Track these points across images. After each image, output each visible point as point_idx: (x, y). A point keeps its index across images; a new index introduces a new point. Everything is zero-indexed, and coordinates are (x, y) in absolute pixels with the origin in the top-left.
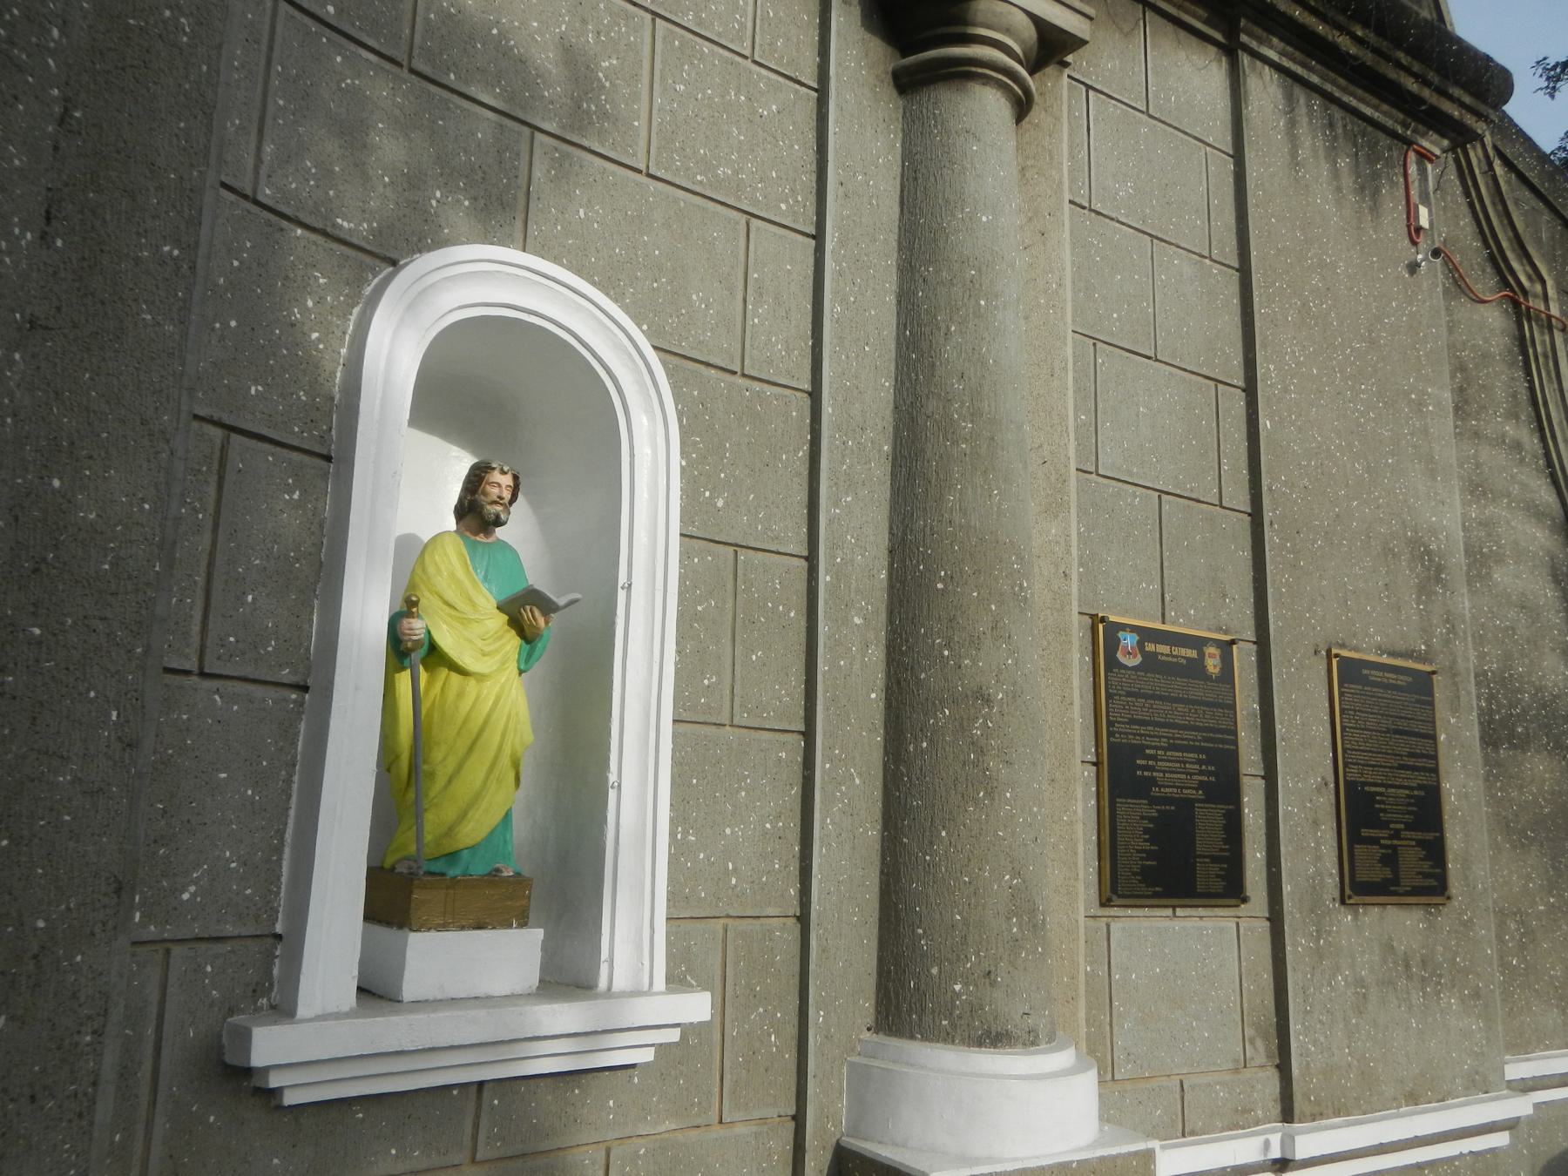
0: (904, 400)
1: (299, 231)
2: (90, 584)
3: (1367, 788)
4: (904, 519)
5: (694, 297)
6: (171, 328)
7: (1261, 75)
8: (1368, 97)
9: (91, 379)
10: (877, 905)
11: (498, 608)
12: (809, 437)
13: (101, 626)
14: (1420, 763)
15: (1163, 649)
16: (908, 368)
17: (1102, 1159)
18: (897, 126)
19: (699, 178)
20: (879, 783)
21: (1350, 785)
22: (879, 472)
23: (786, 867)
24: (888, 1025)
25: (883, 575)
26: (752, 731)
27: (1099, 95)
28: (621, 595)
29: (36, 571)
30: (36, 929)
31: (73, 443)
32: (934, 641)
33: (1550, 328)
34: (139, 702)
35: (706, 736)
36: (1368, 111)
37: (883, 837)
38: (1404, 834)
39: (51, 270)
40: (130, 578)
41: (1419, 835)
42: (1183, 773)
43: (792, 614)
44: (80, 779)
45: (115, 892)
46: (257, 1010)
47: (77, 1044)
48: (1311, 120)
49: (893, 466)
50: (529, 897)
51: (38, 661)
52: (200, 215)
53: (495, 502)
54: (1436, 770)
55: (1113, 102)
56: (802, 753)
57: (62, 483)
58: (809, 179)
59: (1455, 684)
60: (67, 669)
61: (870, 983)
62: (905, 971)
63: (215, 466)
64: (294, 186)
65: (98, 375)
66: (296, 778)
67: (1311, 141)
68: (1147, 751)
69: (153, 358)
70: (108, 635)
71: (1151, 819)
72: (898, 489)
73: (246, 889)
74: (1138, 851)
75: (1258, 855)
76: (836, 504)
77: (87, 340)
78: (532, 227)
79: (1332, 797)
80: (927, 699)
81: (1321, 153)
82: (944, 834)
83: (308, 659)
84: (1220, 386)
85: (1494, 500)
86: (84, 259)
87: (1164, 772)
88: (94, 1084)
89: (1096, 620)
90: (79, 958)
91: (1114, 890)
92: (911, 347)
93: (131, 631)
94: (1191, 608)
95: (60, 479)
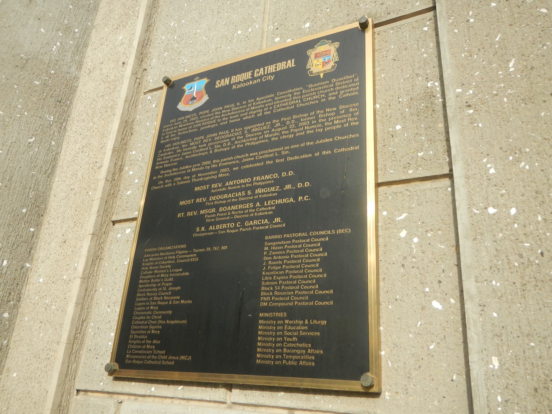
42: (250, 201)
68: (196, 189)
71: (185, 266)
75: (436, 304)
87: (217, 207)
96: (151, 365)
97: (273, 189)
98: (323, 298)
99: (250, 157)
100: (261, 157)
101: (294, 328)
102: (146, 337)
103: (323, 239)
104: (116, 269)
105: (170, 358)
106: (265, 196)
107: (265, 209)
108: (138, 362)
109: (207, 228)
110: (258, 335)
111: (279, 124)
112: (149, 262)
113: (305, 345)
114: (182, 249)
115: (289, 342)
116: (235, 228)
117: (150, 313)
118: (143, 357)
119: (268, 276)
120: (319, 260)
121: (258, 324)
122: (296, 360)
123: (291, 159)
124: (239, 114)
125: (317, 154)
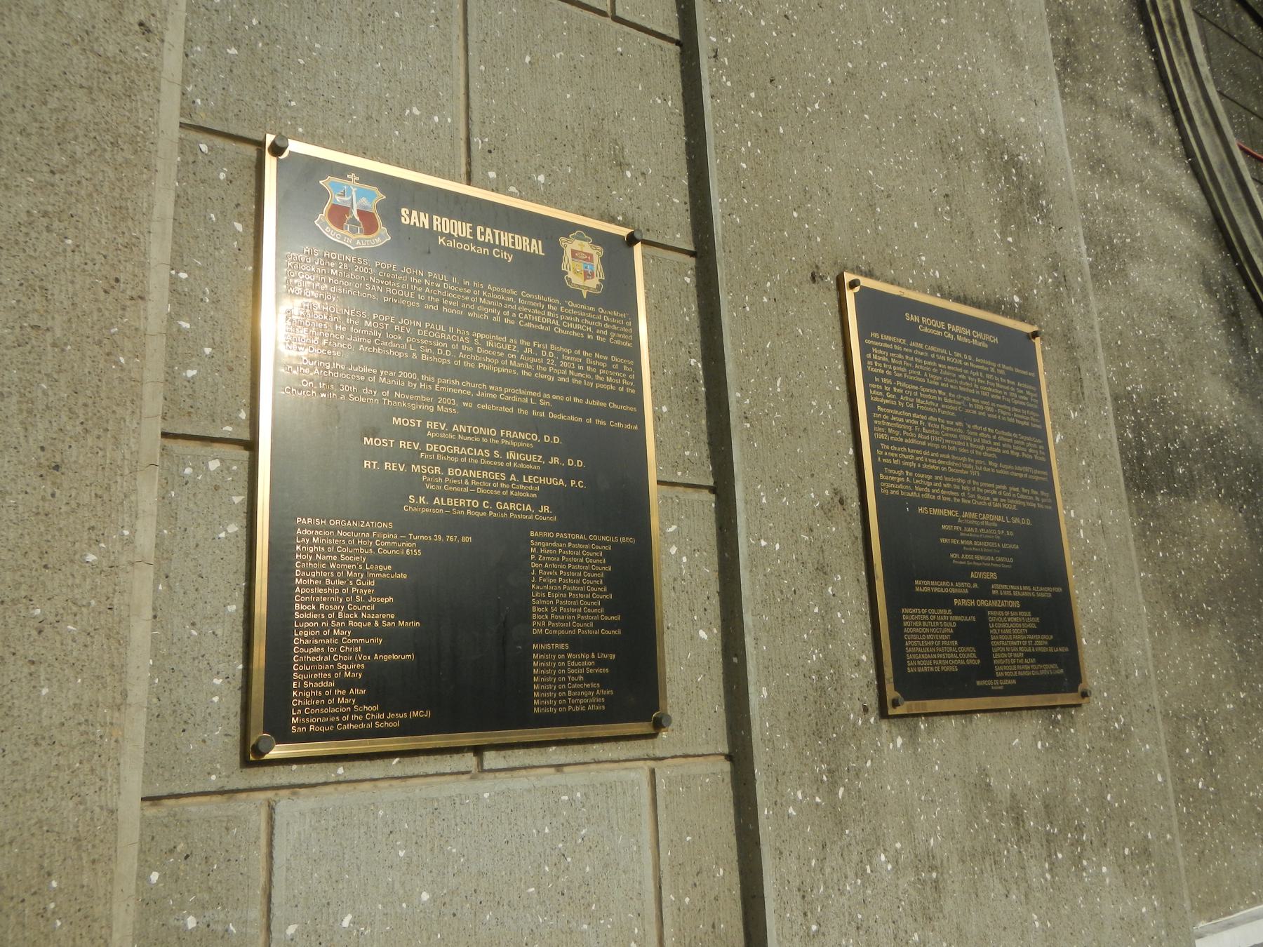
14: (1022, 472)
41: (1026, 591)
42: (499, 469)
59: (1074, 360)
71: (398, 563)
75: (703, 634)
79: (856, 525)
85: (1122, 182)
94: (538, 170)
96: (352, 730)
97: (533, 458)
98: (610, 625)
99: (488, 391)
100: (508, 398)
101: (578, 664)
102: (332, 684)
103: (605, 548)
104: (197, 546)
105: (391, 716)
106: (522, 466)
107: (525, 488)
108: (323, 729)
109: (430, 496)
110: (532, 675)
111: (529, 351)
112: (311, 545)
113: (594, 685)
114: (384, 531)
115: (574, 682)
116: (481, 509)
117: (335, 641)
118: (332, 719)
119: (540, 591)
120: (602, 575)
121: (532, 660)
122: (583, 704)
123: (554, 416)
124: (461, 301)
125: (589, 421)
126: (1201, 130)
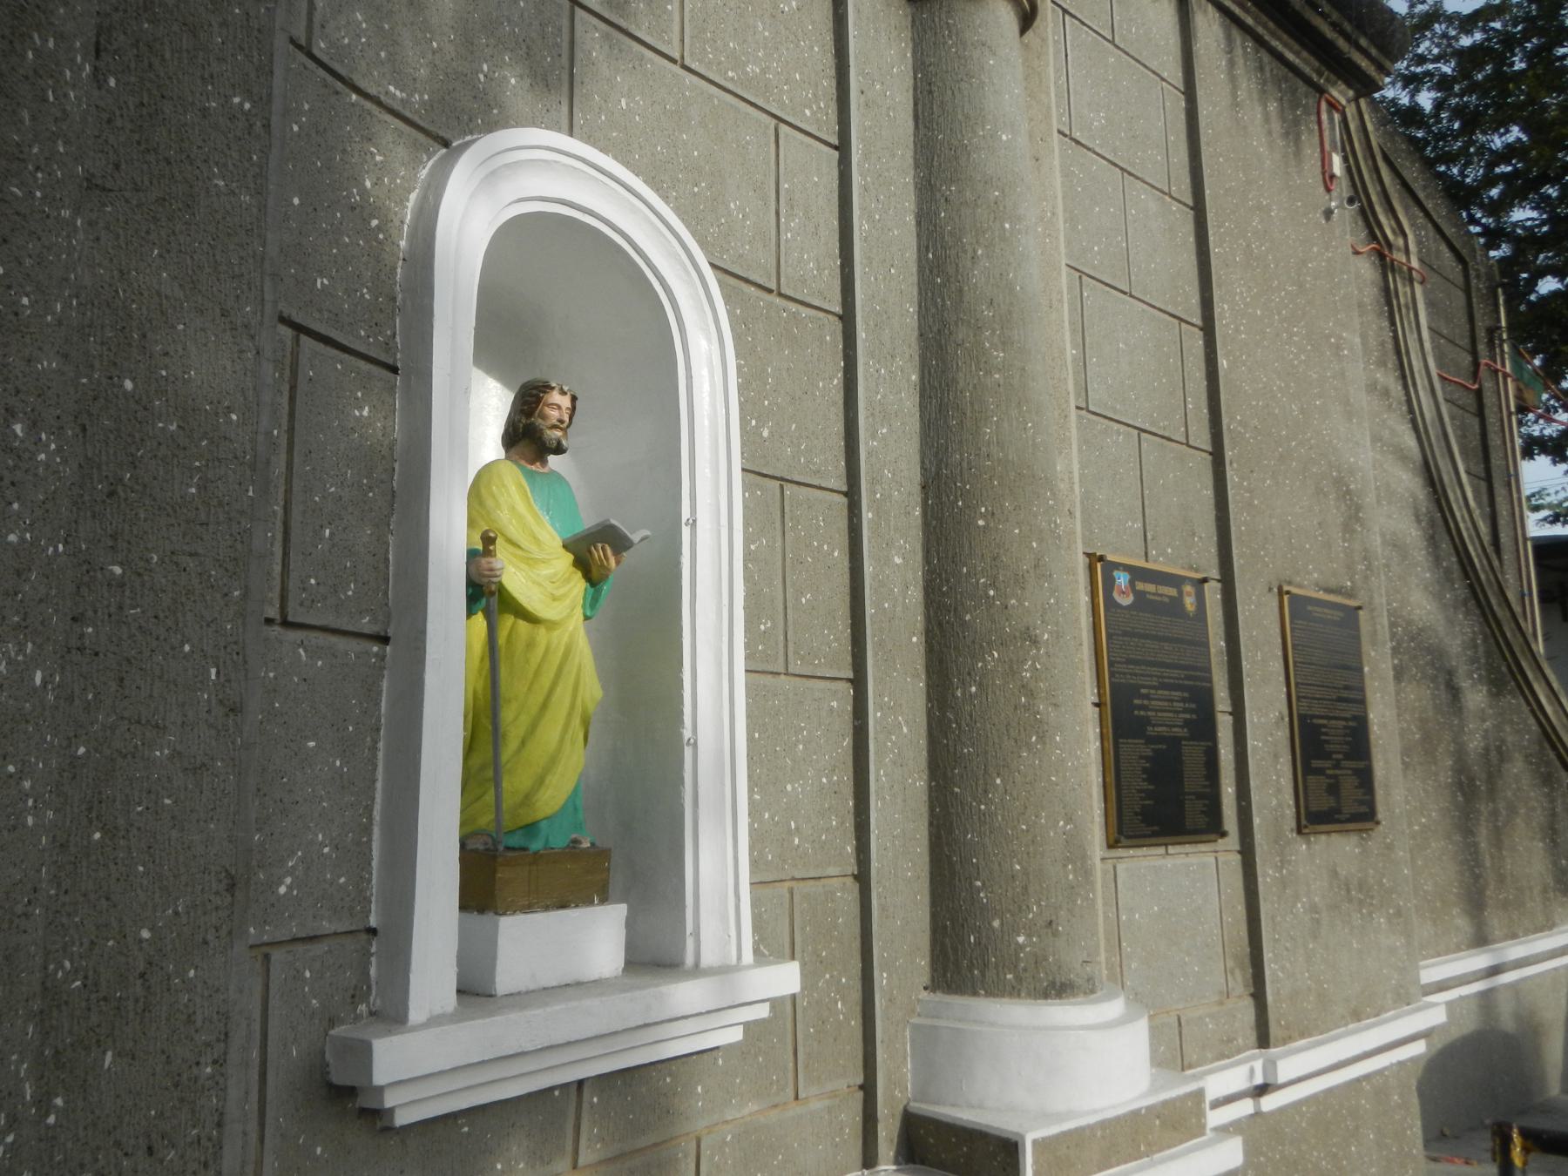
0: (930, 328)
1: (354, 97)
2: (175, 511)
3: (1315, 721)
4: (937, 453)
5: (732, 206)
6: (248, 198)
7: (1205, 11)
8: (1292, 42)
9: (160, 255)
10: (927, 859)
11: (565, 546)
12: (842, 364)
13: (191, 564)
15: (1150, 588)
16: (933, 293)
17: (1165, 1103)
18: (907, 34)
19: (730, 74)
20: (923, 731)
21: (1302, 718)
22: (909, 402)
23: (843, 823)
24: (946, 983)
25: (918, 513)
26: (804, 680)
27: (1074, 20)
28: (686, 532)
29: (111, 494)
30: (141, 941)
31: (144, 336)
32: (978, 582)
33: (1411, 280)
34: (241, 657)
35: (765, 686)
36: (1290, 56)
37: (930, 787)
38: (1345, 763)
39: (105, 116)
40: (220, 504)
43: (836, 554)
44: (179, 753)
45: (227, 890)
46: (358, 1018)
47: (196, 1079)
48: (1246, 62)
49: (922, 396)
50: (609, 870)
51: (121, 608)
52: (271, 62)
53: (554, 427)
54: (1362, 702)
55: (1085, 28)
56: (851, 701)
57: (136, 386)
58: (828, 84)
60: (156, 617)
61: (924, 940)
62: (963, 926)
63: (287, 373)
64: (346, 41)
65: (168, 252)
66: (381, 745)
67: (1248, 86)
69: (229, 235)
70: (200, 574)
72: (929, 420)
73: (339, 878)
74: (1140, 791)
76: (873, 436)
77: (153, 207)
78: (578, 115)
79: (1287, 731)
80: (973, 642)
81: (1255, 96)
82: (998, 781)
83: (387, 605)
84: (1183, 325)
86: (142, 104)
87: (1156, 711)
88: (219, 1125)
89: (1094, 559)
90: (192, 974)
91: (1120, 832)
92: (935, 271)
93: (227, 570)
95: (133, 380)
126: (1421, 394)
